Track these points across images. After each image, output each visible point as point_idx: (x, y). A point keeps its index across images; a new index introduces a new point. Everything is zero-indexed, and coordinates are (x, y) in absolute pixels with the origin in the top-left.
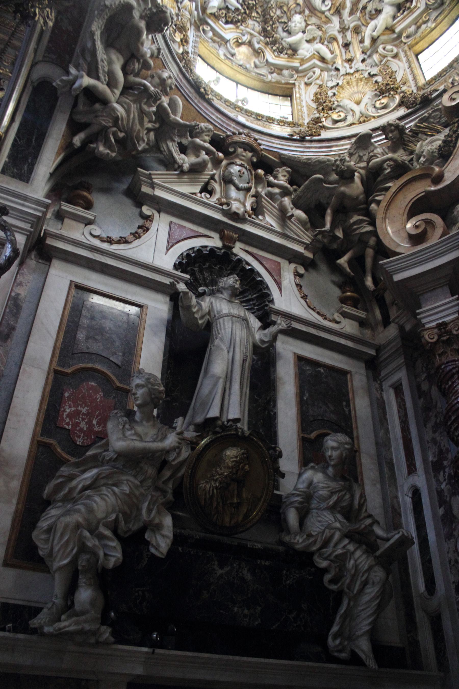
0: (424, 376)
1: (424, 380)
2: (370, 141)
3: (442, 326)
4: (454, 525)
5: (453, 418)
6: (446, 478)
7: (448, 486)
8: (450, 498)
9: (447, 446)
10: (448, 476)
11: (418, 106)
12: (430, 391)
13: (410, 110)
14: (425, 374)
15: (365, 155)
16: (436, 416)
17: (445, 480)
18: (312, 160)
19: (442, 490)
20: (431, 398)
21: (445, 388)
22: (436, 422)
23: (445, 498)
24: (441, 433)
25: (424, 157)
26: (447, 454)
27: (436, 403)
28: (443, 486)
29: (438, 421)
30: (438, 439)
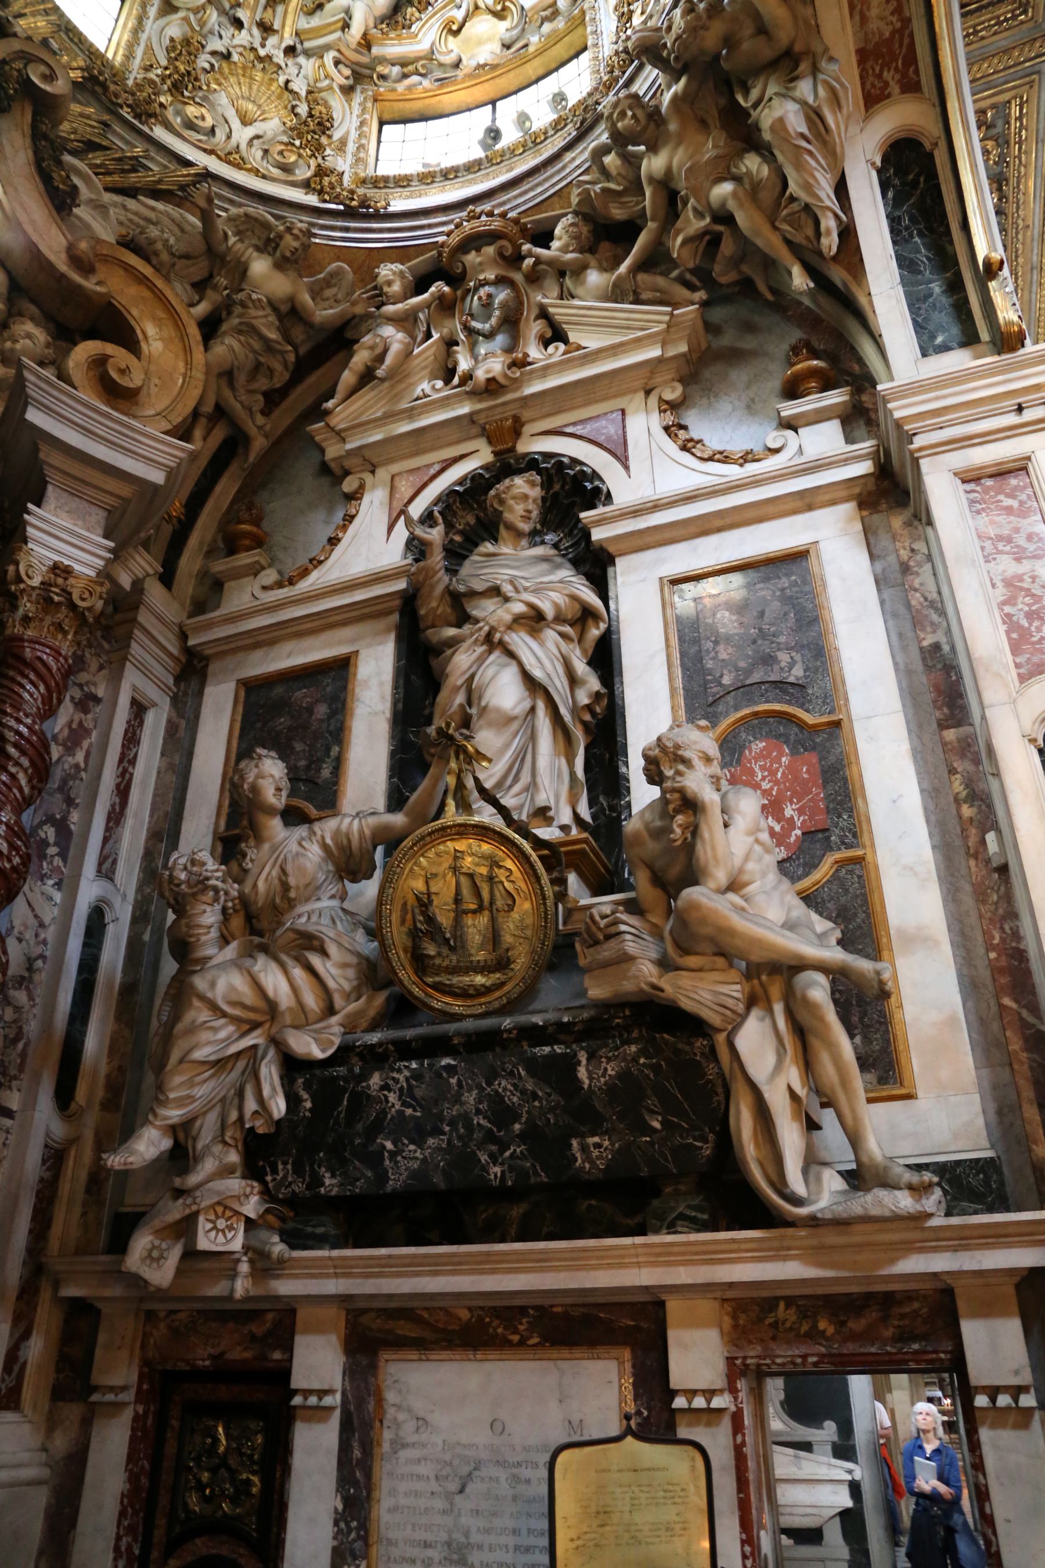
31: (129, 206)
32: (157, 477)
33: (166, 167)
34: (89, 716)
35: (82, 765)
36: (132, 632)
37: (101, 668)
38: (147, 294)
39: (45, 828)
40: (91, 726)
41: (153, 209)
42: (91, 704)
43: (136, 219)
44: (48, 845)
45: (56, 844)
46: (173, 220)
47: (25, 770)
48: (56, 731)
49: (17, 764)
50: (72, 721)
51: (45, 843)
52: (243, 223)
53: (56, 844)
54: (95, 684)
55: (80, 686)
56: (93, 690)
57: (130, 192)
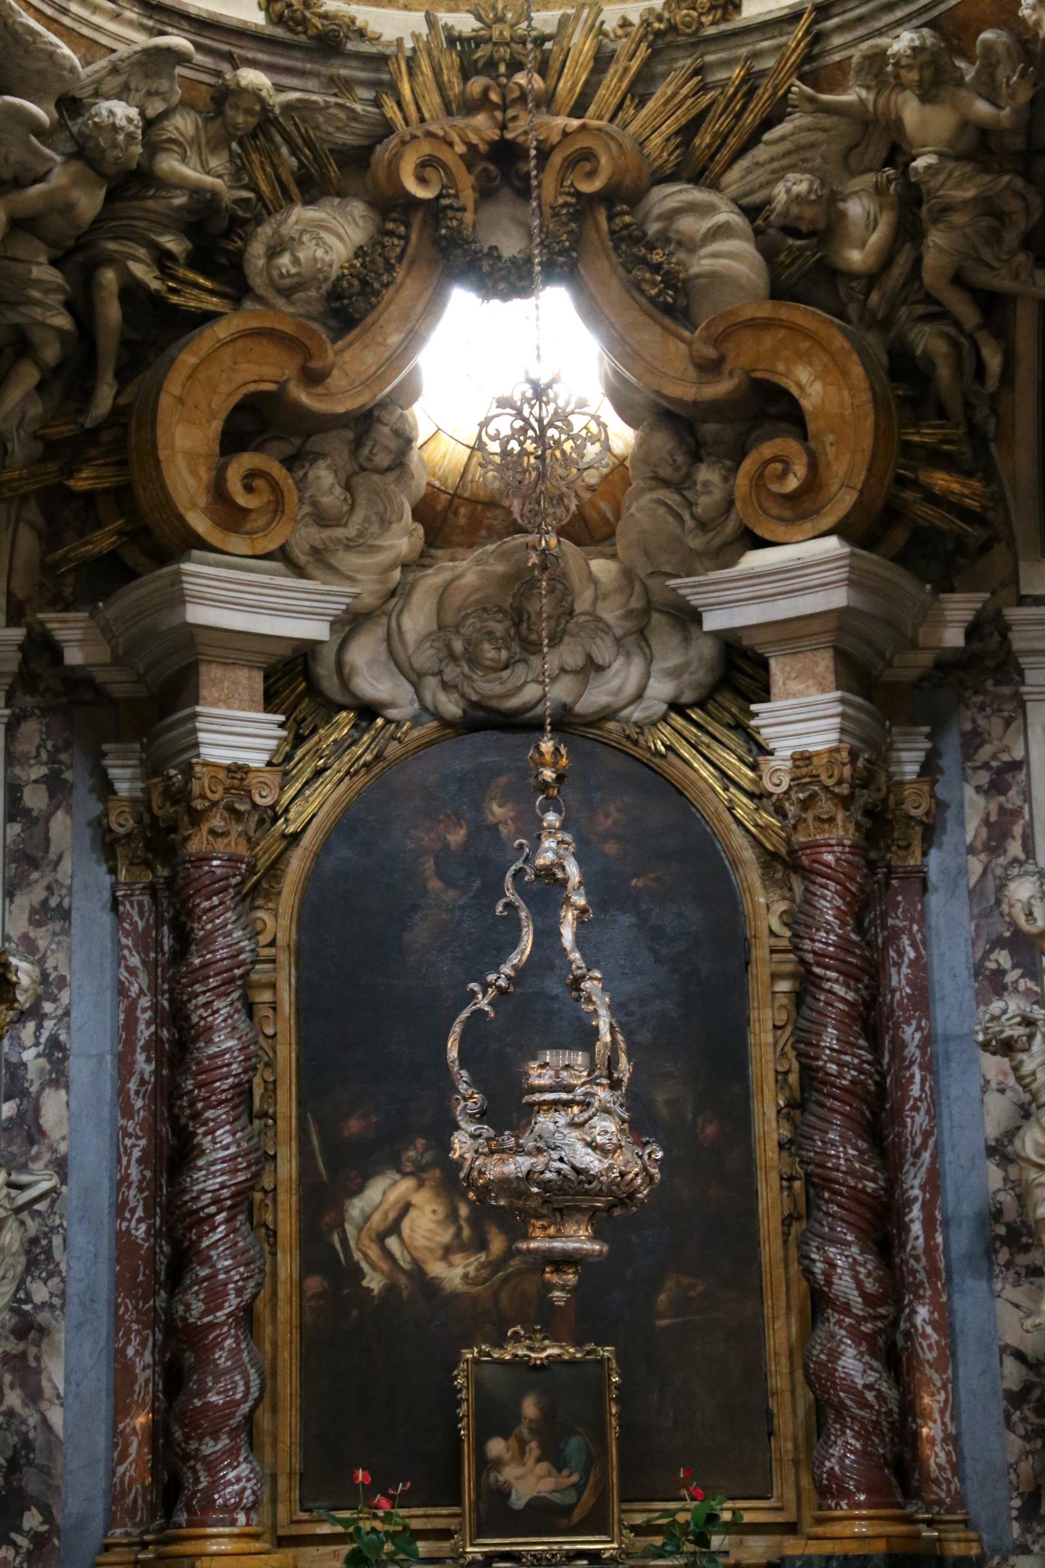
0: (38, 772)
1: (36, 781)
2: (174, 68)
3: (238, 770)
4: (34, 1150)
5: (213, 982)
6: (43, 1040)
7: (42, 1061)
8: (42, 1088)
9: (64, 971)
10: (48, 1040)
11: (303, 38)
12: (48, 821)
13: (279, 32)
14: (44, 770)
15: (137, 90)
16: (49, 888)
17: (37, 1044)
18: (39, 39)
19: (24, 1065)
20: (47, 841)
21: (199, 904)
22: (45, 903)
23: (27, 1085)
24: (54, 934)
25: (296, 261)
26: (60, 989)
27: (60, 857)
28: (28, 1056)
29: (53, 902)
30: (42, 944)
31: (761, 159)
32: (838, 598)
33: (778, 48)
34: (1012, 793)
35: (1022, 856)
36: (1019, 664)
37: (1008, 723)
38: (782, 333)
39: (993, 956)
40: (1019, 803)
41: (782, 138)
42: (1009, 777)
43: (776, 165)
44: (1003, 972)
45: (1015, 966)
46: (809, 130)
47: (836, 981)
48: (969, 839)
49: (828, 980)
50: (988, 815)
51: (1001, 972)
52: (870, 66)
53: (1015, 966)
54: (1007, 749)
55: (986, 766)
56: (1006, 757)
57: (753, 140)
